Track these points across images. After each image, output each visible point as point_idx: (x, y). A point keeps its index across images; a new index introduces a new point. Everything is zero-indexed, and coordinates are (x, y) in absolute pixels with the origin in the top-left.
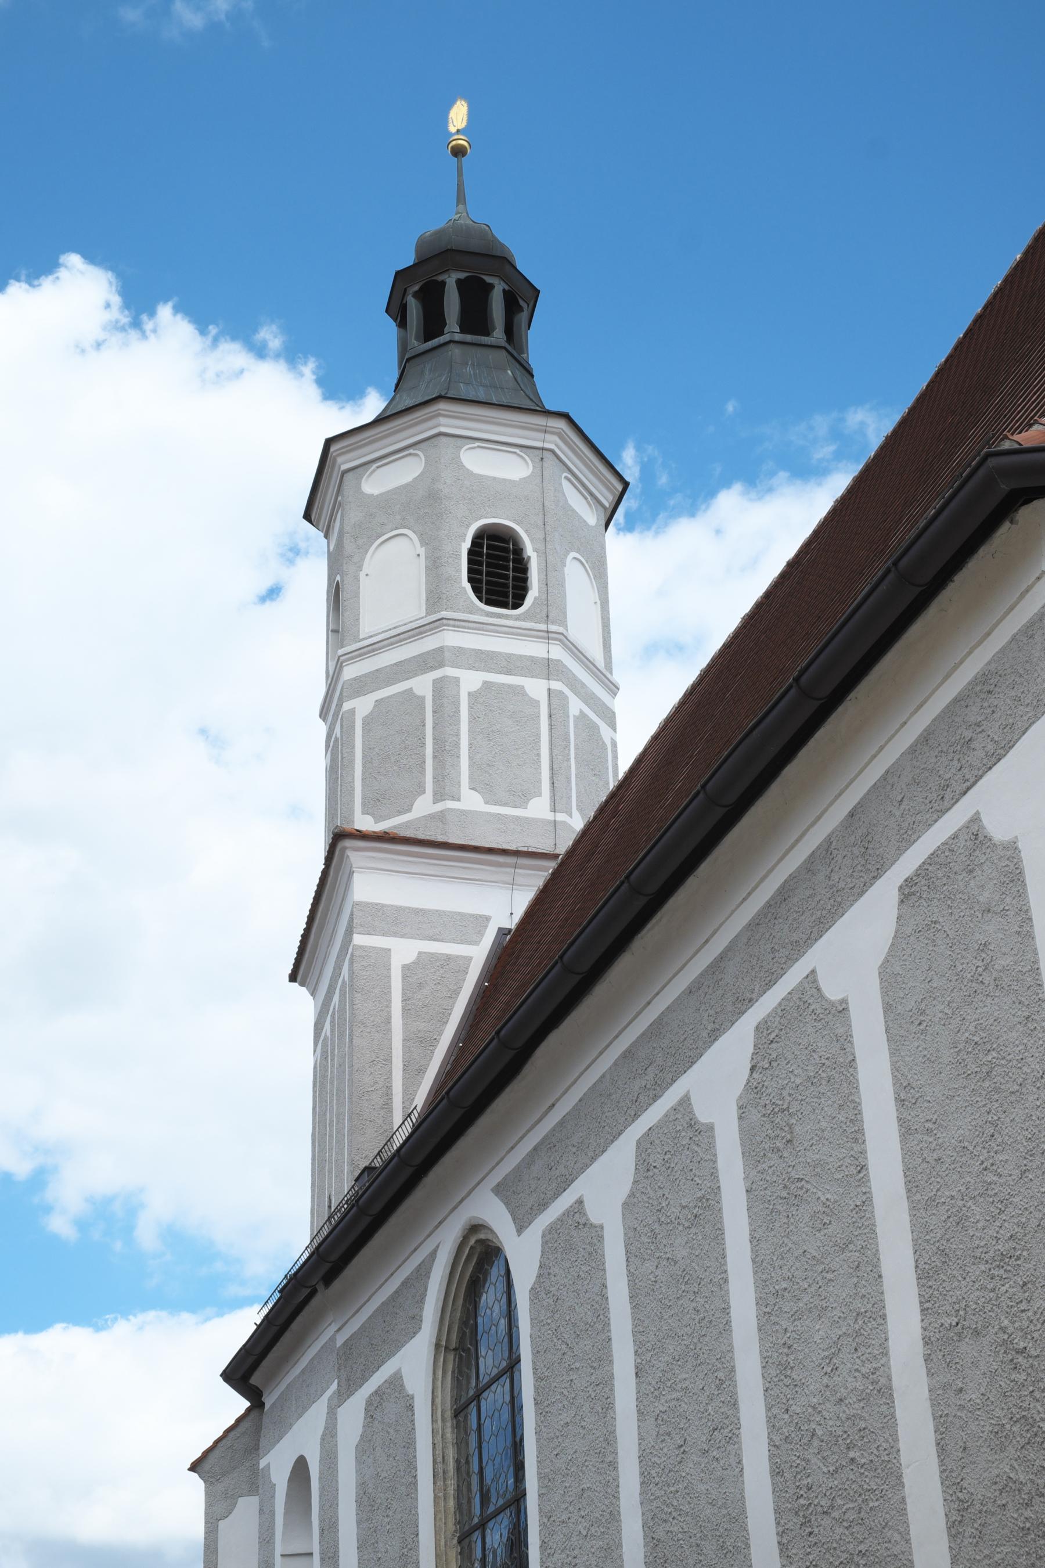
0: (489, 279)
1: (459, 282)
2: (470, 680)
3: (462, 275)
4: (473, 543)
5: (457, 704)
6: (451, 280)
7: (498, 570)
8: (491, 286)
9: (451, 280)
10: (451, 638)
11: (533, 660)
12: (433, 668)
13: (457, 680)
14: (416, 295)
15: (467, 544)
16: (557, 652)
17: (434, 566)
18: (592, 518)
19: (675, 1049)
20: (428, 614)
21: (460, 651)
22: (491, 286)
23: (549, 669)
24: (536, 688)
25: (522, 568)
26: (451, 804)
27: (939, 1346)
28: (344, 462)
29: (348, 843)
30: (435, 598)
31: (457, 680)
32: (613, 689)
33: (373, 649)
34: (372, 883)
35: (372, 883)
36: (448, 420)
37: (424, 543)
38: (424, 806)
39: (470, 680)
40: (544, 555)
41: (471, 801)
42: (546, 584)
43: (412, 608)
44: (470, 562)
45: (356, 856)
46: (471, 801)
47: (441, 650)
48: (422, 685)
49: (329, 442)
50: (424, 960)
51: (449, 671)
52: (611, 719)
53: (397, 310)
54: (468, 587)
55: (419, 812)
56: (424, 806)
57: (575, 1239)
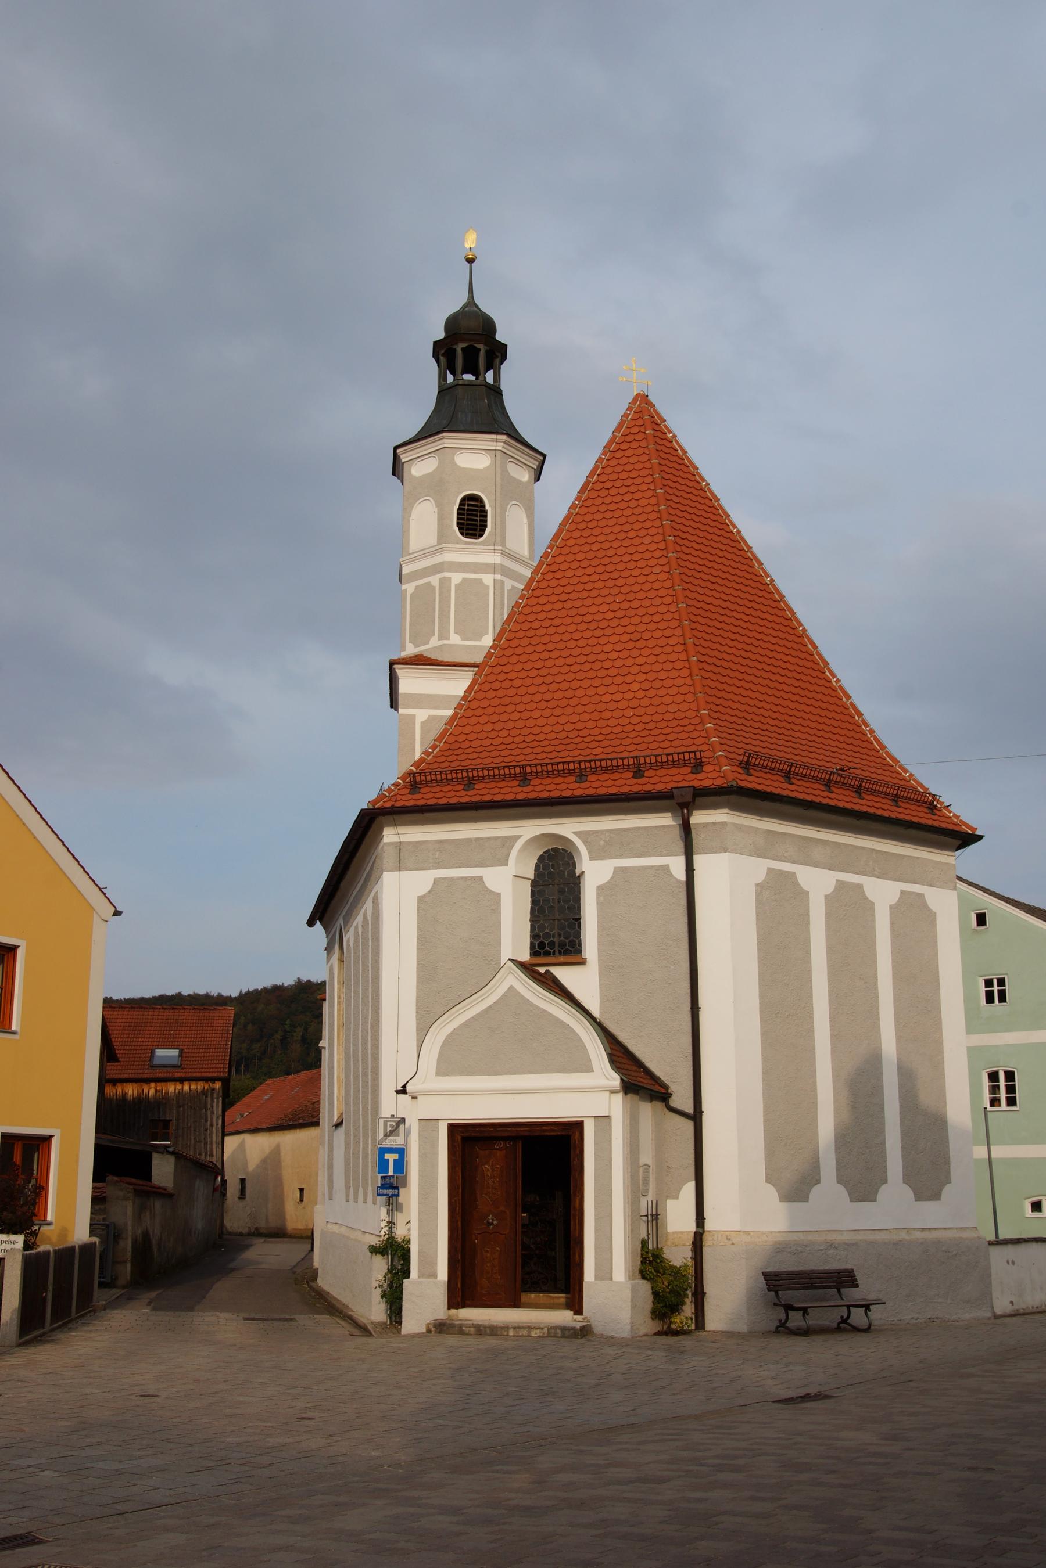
0: (478, 346)
1: (463, 349)
2: (456, 578)
3: (464, 345)
4: (461, 504)
5: (449, 591)
6: (459, 347)
7: (472, 518)
8: (480, 350)
9: (459, 347)
10: (449, 557)
11: (487, 565)
12: (440, 572)
13: (450, 579)
14: (443, 355)
15: (457, 506)
16: (498, 559)
17: (441, 518)
18: (525, 476)
20: (439, 544)
21: (451, 563)
22: (480, 350)
23: (493, 568)
24: (488, 579)
25: (484, 514)
26: (446, 642)
28: (404, 458)
29: (395, 666)
30: (442, 537)
31: (450, 579)
33: (414, 560)
34: (410, 682)
35: (410, 682)
36: (449, 440)
37: (437, 506)
38: (434, 642)
39: (456, 578)
40: (494, 508)
41: (455, 639)
42: (494, 524)
43: (433, 540)
44: (458, 514)
45: (401, 671)
46: (455, 639)
47: (442, 563)
48: (434, 580)
49: (396, 448)
51: (447, 574)
53: (436, 356)
54: (456, 529)
55: (431, 646)
56: (434, 642)
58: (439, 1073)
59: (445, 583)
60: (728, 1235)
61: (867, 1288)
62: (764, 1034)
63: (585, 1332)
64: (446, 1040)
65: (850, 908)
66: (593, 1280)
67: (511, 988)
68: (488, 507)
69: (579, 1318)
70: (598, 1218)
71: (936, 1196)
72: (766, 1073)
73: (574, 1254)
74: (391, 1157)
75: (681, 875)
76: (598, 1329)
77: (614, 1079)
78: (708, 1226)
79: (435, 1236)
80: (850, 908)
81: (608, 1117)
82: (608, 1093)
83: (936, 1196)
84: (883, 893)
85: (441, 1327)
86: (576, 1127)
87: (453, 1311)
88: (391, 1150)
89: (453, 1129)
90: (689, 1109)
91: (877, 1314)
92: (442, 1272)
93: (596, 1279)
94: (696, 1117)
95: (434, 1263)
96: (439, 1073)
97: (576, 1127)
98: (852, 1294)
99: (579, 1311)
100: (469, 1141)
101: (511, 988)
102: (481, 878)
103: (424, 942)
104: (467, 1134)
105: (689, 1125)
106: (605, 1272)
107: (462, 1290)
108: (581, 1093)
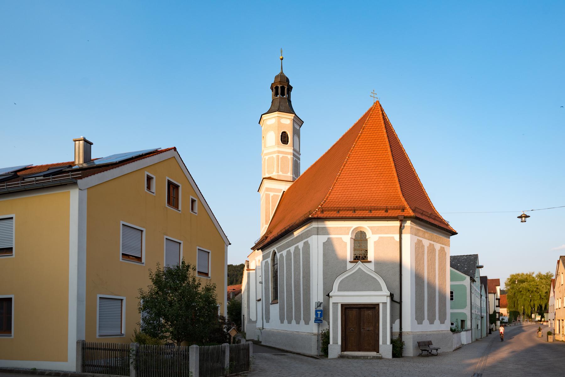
2: (281, 155)
19: (289, 245)
27: (303, 277)
32: (300, 154)
39: (281, 155)
50: (274, 195)
52: (299, 159)
57: (281, 255)
59: (278, 156)
60: (408, 333)
61: (434, 345)
62: (416, 282)
63: (380, 358)
65: (432, 249)
68: (289, 136)
71: (444, 323)
72: (416, 292)
74: (319, 313)
75: (398, 240)
76: (384, 356)
78: (403, 330)
80: (432, 249)
83: (444, 323)
84: (438, 246)
85: (341, 357)
86: (378, 305)
88: (319, 311)
89: (342, 305)
90: (398, 300)
91: (439, 351)
92: (340, 342)
94: (400, 303)
97: (378, 305)
98: (431, 346)
99: (378, 352)
100: (346, 308)
102: (341, 238)
103: (325, 255)
105: (398, 305)
106: (385, 342)
107: (344, 347)
108: (380, 297)
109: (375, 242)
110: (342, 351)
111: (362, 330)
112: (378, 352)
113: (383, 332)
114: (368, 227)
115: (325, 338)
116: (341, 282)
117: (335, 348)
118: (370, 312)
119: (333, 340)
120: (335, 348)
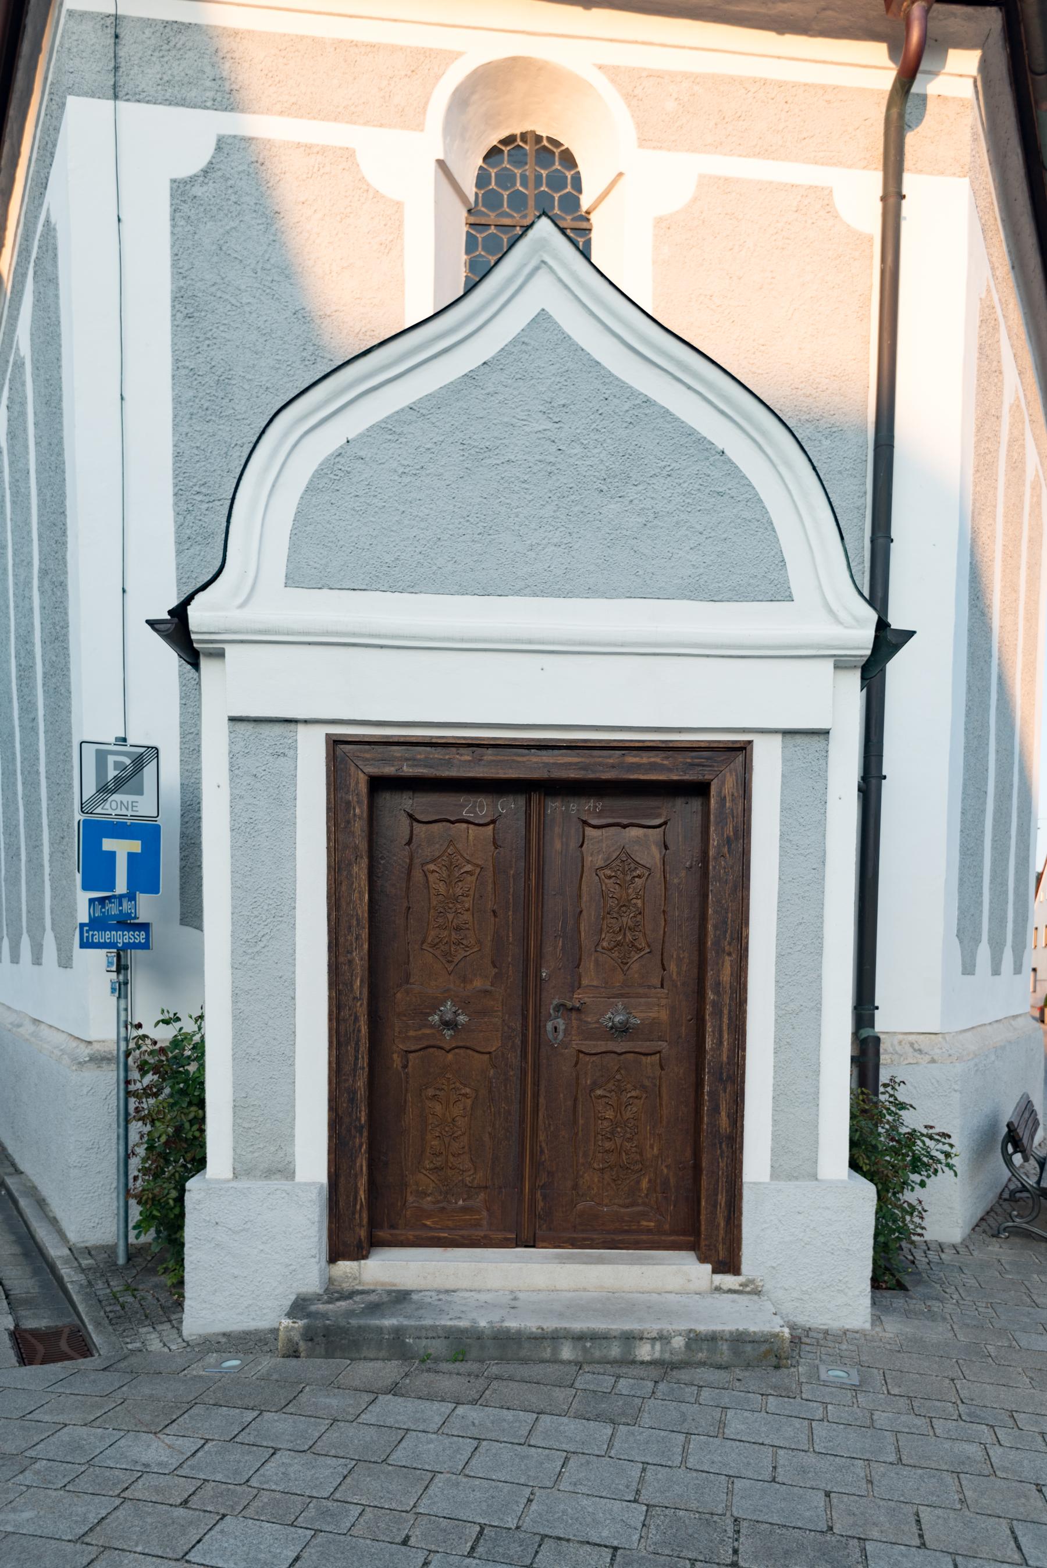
58: (292, 580)
64: (318, 474)
66: (766, 1178)
67: (542, 318)
69: (728, 1281)
70: (784, 1015)
73: (715, 1110)
77: (859, 622)
79: (289, 1060)
81: (826, 732)
82: (830, 664)
86: (737, 753)
87: (345, 1266)
89: (339, 750)
93: (775, 1175)
95: (284, 1135)
96: (292, 580)
97: (737, 753)
99: (727, 1261)
100: (387, 787)
101: (542, 318)
104: (389, 770)
109: (663, 225)
110: (346, 1240)
111: (556, 1025)
112: (727, 1261)
113: (780, 1045)
114: (611, 72)
115: (166, 1104)
116: (332, 474)
117: (258, 1237)
118: (640, 840)
119: (241, 1132)
120: (258, 1237)
